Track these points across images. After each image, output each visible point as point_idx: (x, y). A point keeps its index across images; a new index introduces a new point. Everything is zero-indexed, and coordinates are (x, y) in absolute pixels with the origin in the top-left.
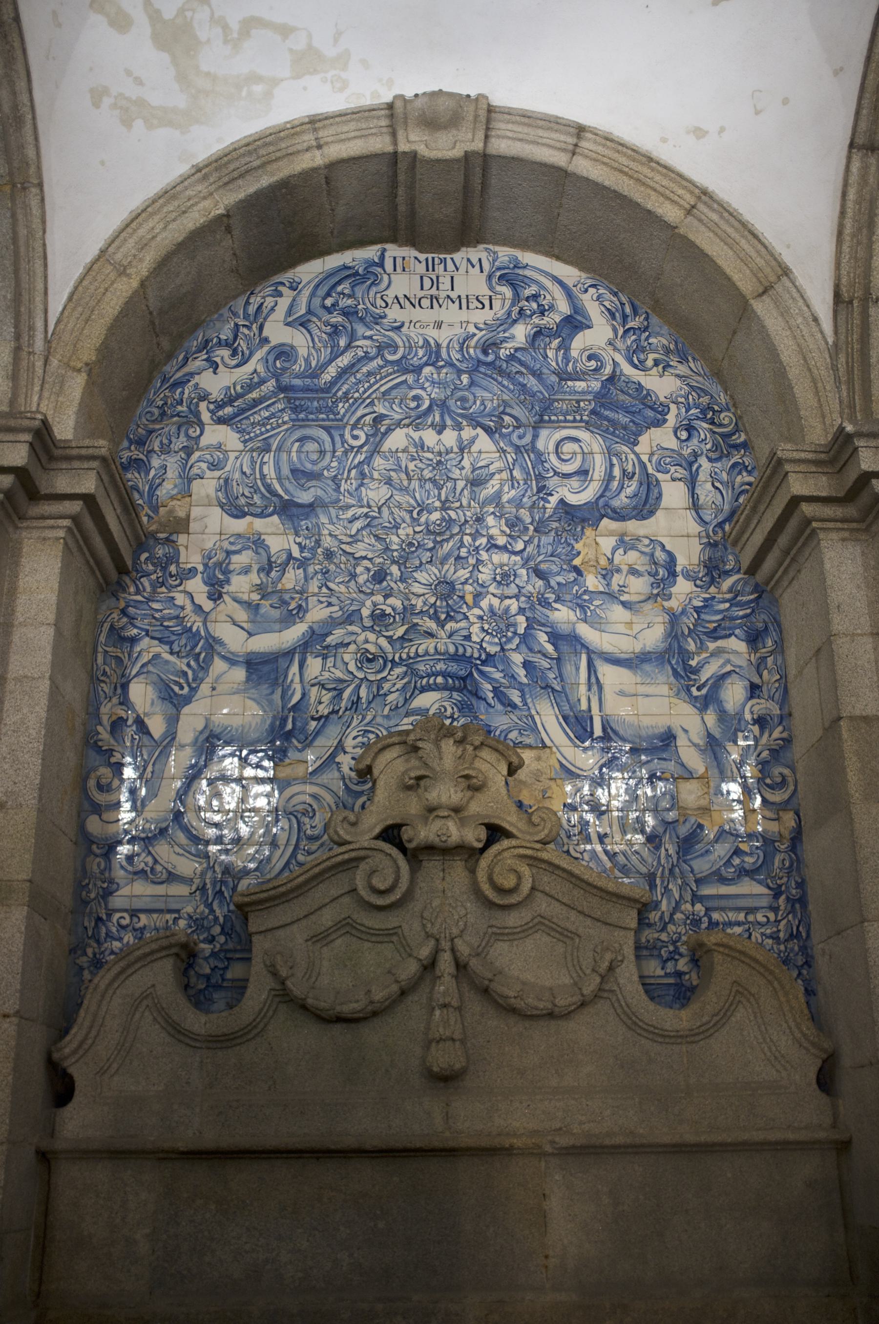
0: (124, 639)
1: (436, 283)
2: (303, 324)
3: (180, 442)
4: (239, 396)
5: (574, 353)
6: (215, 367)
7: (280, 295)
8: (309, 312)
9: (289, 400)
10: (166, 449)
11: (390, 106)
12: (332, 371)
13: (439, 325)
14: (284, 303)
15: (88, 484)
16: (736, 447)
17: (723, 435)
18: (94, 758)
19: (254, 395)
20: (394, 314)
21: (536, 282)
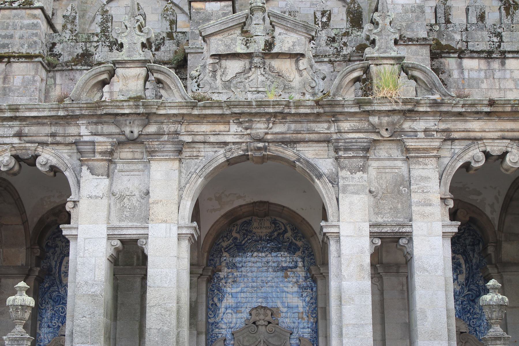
0: (212, 290)
1: (261, 224)
2: (238, 233)
3: (219, 256)
4: (228, 247)
5: (285, 238)
6: (224, 241)
7: (234, 227)
8: (240, 230)
9: (237, 247)
10: (217, 257)
11: (253, 203)
12: (243, 242)
13: (262, 232)
14: (235, 228)
15: (210, 274)
16: (312, 255)
17: (310, 253)
18: (209, 310)
19: (231, 247)
20: (254, 230)
21: (279, 223)
